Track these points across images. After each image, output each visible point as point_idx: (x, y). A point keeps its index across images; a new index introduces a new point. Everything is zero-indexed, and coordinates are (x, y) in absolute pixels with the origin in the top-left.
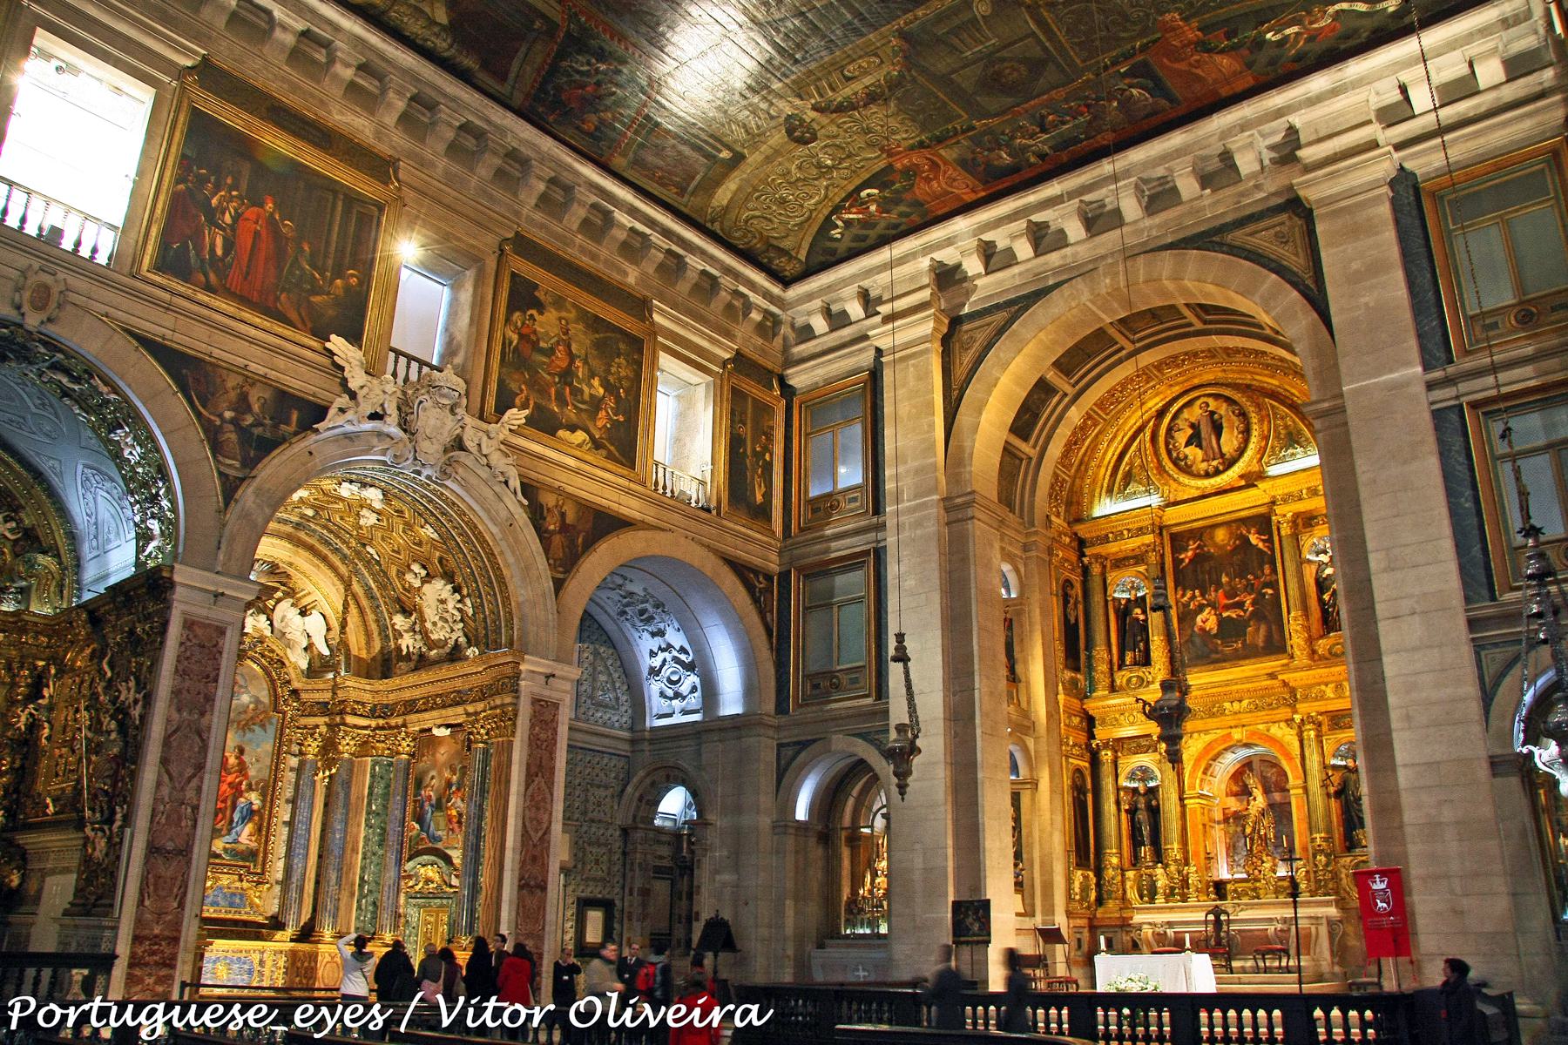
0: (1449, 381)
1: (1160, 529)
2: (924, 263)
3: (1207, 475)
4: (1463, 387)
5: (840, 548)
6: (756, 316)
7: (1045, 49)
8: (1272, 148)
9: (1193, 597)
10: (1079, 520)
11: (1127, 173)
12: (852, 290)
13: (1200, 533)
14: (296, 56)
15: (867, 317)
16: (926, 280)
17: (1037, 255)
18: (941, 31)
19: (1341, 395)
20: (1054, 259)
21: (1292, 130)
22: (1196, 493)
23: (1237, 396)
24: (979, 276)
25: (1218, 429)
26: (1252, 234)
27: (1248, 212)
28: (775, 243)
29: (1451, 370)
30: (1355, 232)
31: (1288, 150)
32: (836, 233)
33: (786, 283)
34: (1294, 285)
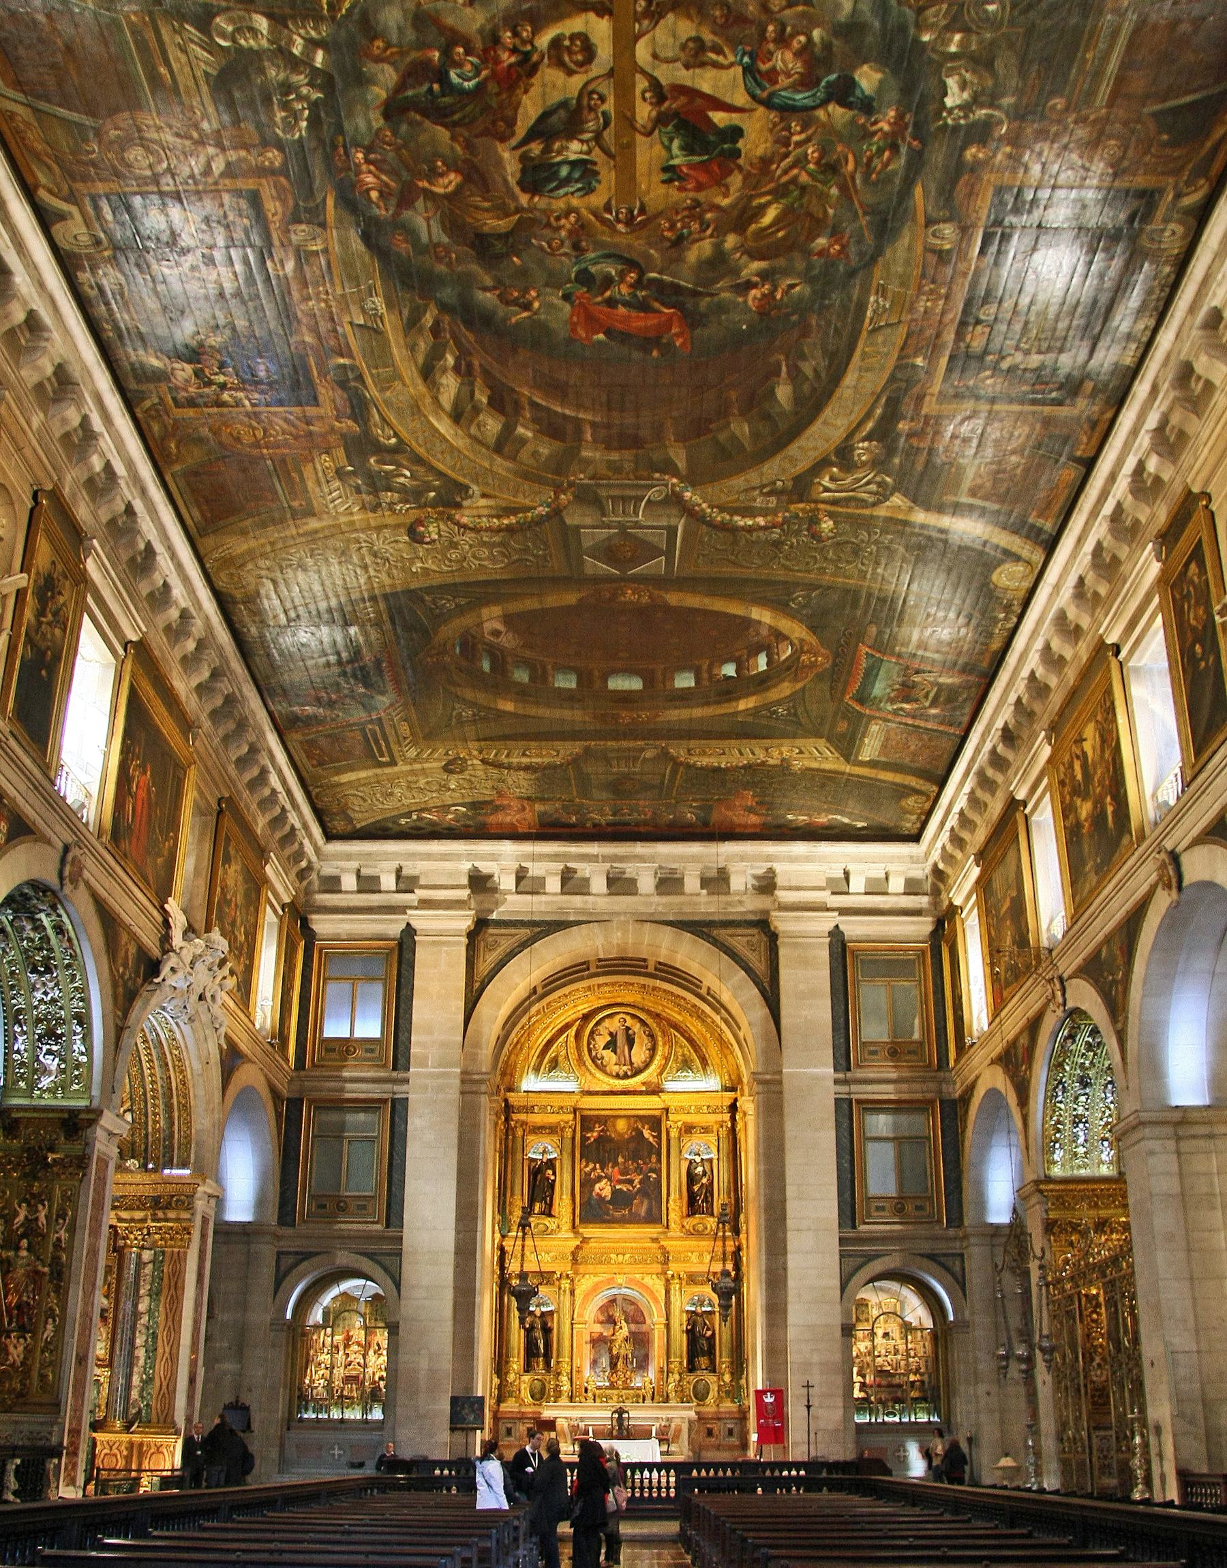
0: (846, 1082)
1: (575, 1110)
2: (467, 866)
3: (618, 1076)
4: (854, 1088)
5: (354, 1091)
6: (304, 864)
7: (662, 783)
8: (756, 877)
9: (594, 1169)
10: (510, 1089)
11: (652, 859)
12: (395, 864)
13: (604, 1120)
14: (168, 629)
15: (398, 891)
16: (465, 881)
17: (563, 893)
18: (610, 755)
19: (780, 1072)
20: (577, 901)
21: (771, 870)
22: (606, 1088)
23: (649, 1021)
24: (509, 892)
25: (630, 1042)
26: (732, 936)
27: (731, 918)
28: (350, 812)
29: (849, 1075)
30: (805, 962)
31: (767, 885)
32: (403, 821)
33: (329, 836)
34: (756, 984)
